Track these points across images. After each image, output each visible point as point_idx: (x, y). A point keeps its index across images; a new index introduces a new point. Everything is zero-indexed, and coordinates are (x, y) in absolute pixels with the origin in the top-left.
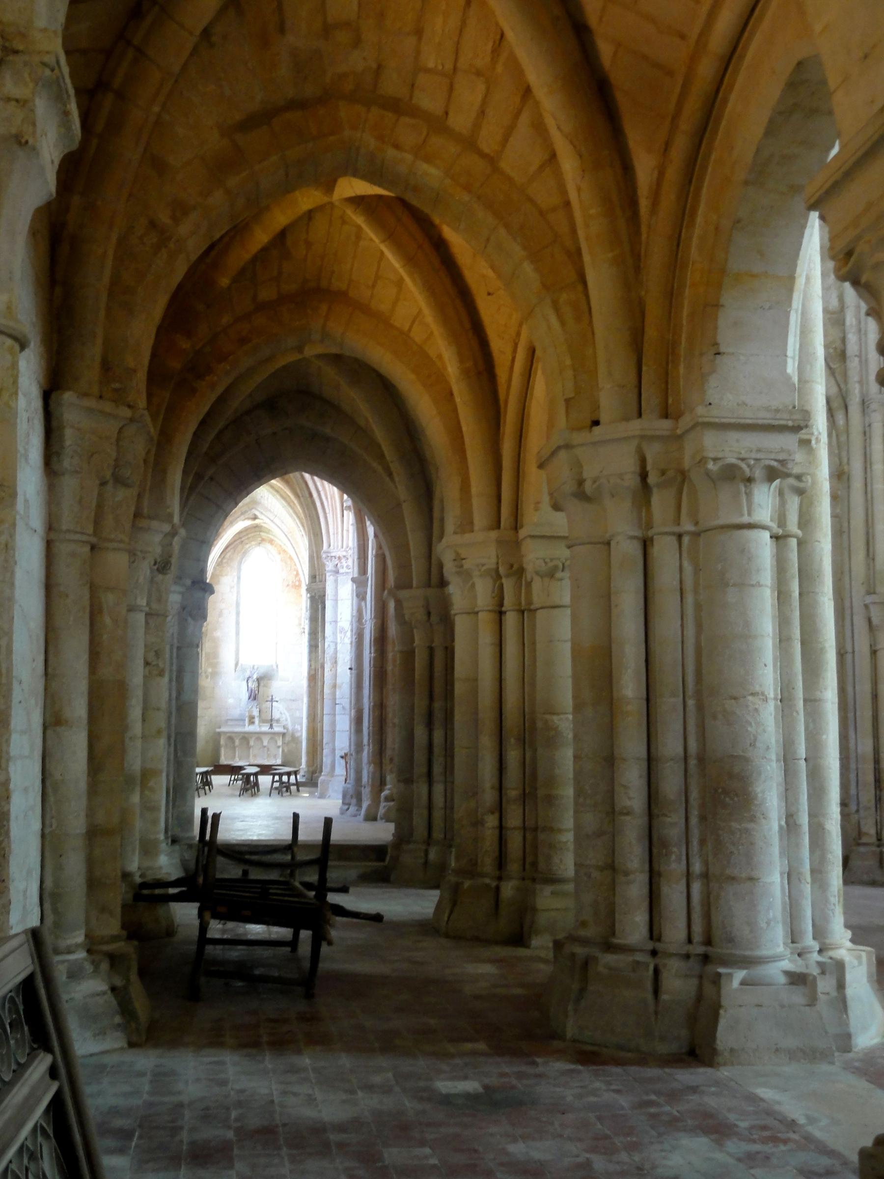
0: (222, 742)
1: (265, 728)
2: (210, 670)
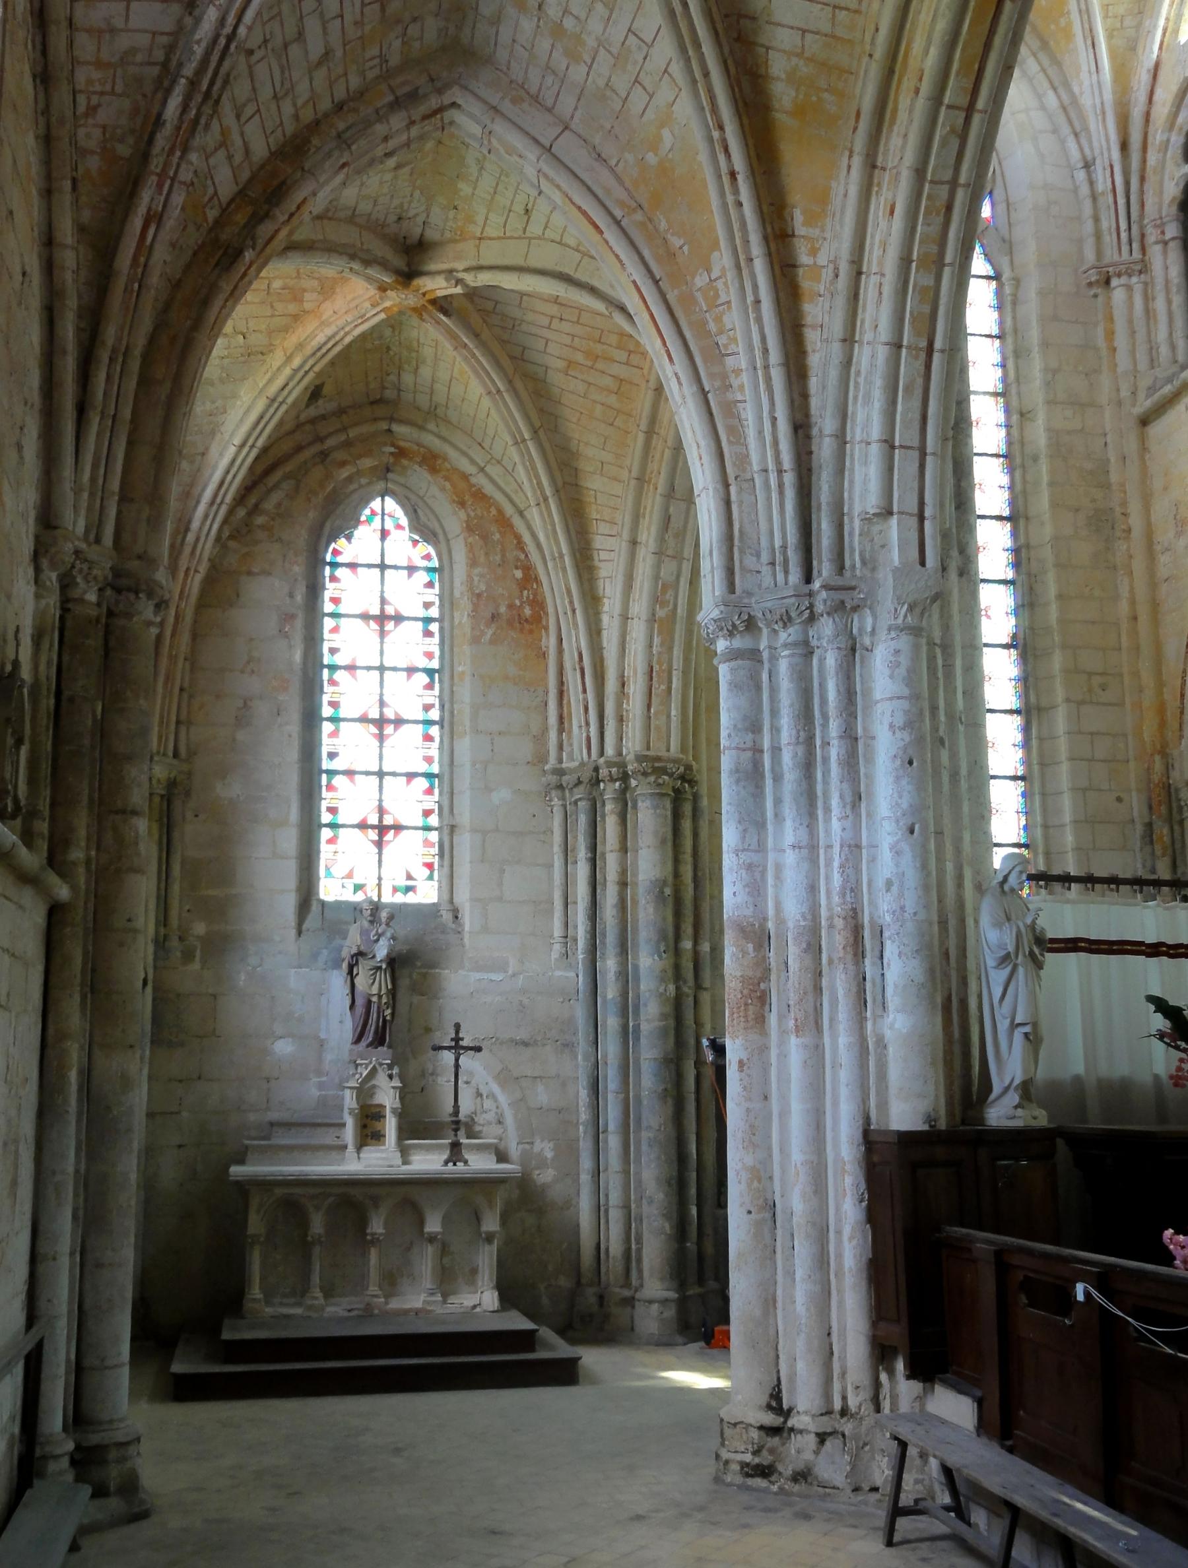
0: (255, 1224)
1: (428, 1161)
2: (200, 928)
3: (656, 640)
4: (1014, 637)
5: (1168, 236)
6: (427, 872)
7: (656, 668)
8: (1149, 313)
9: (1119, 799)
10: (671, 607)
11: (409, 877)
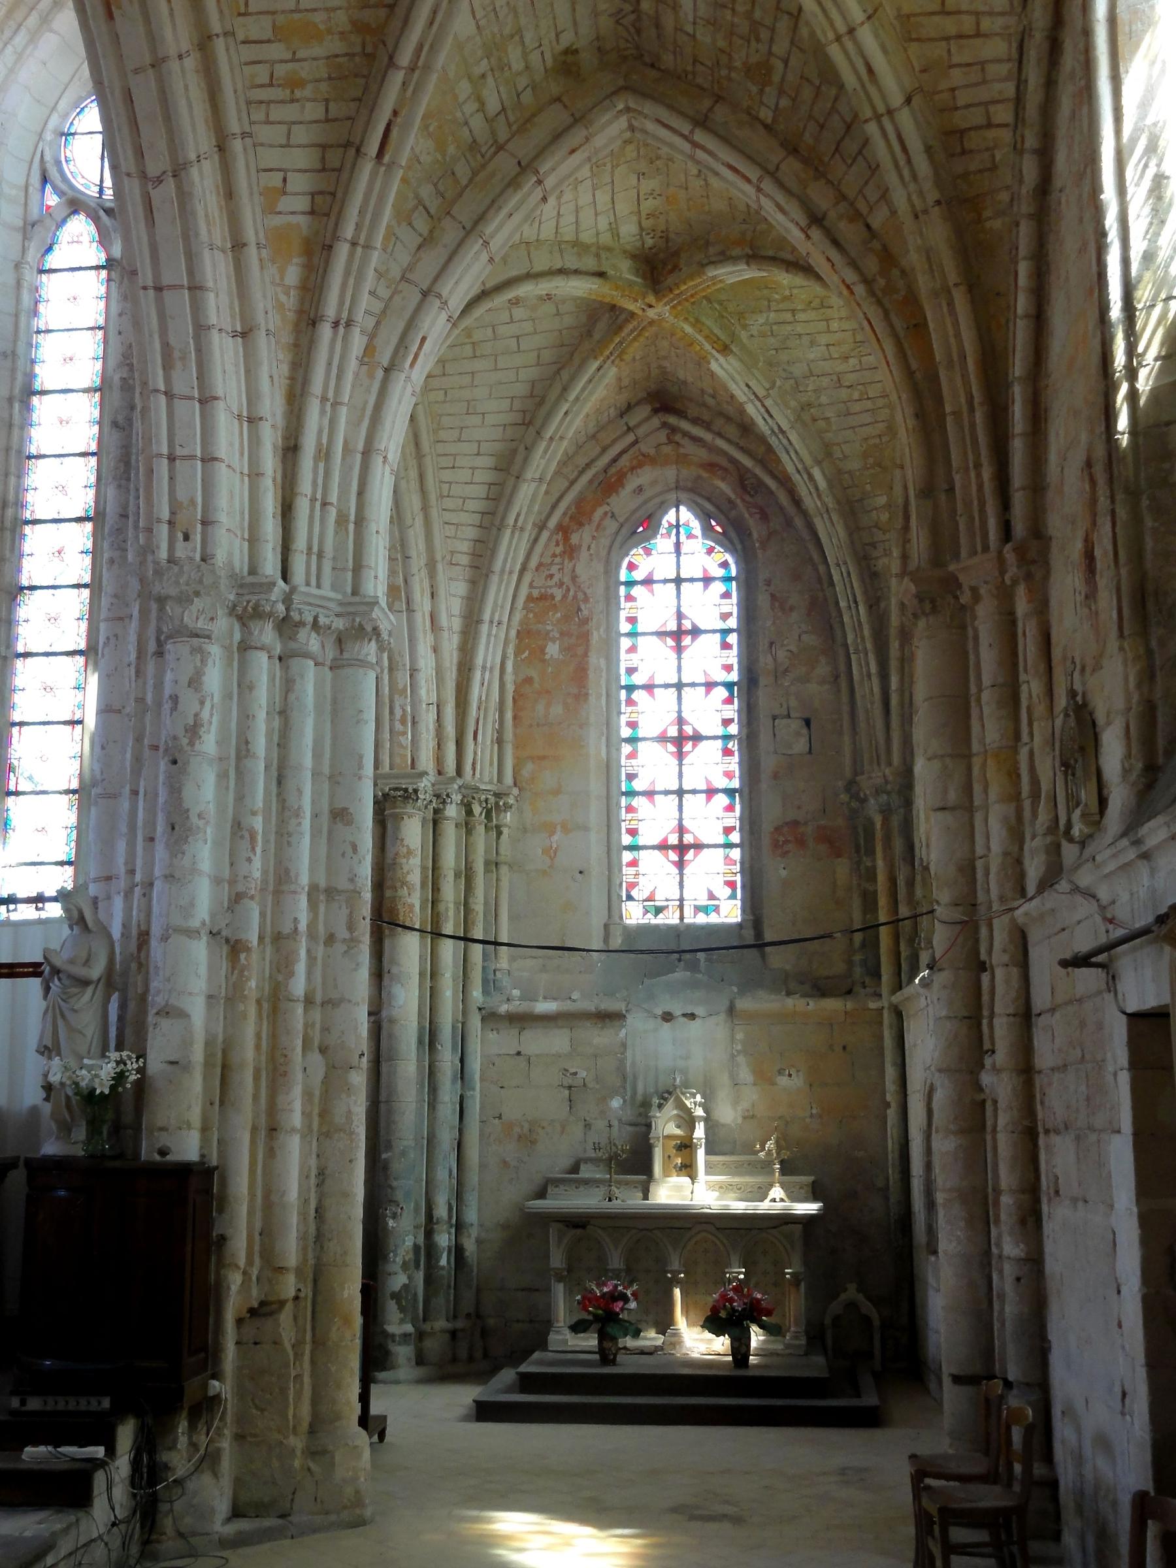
6: (728, 891)
11: (712, 896)
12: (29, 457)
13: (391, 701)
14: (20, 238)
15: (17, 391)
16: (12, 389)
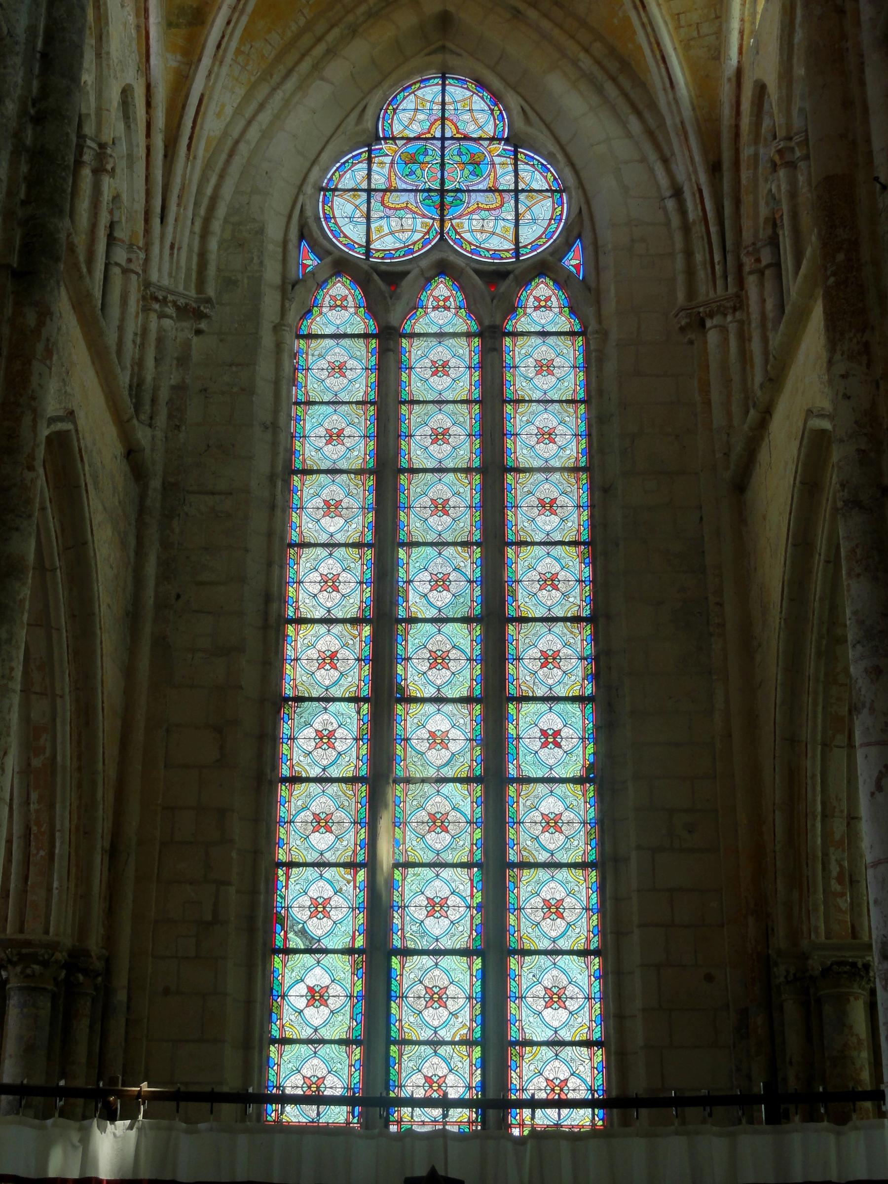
3: (34, 796)
4: (590, 768)
5: (764, 262)
7: (34, 829)
8: (744, 355)
9: (709, 978)
10: (48, 754)
12: (291, 545)
13: (825, 854)
14: (278, 297)
15: (280, 468)
16: (273, 466)
